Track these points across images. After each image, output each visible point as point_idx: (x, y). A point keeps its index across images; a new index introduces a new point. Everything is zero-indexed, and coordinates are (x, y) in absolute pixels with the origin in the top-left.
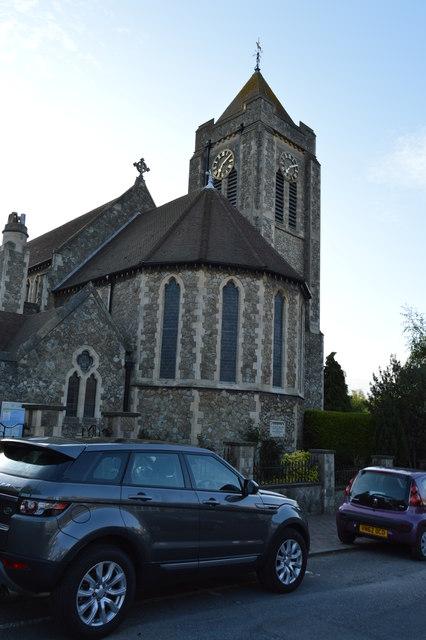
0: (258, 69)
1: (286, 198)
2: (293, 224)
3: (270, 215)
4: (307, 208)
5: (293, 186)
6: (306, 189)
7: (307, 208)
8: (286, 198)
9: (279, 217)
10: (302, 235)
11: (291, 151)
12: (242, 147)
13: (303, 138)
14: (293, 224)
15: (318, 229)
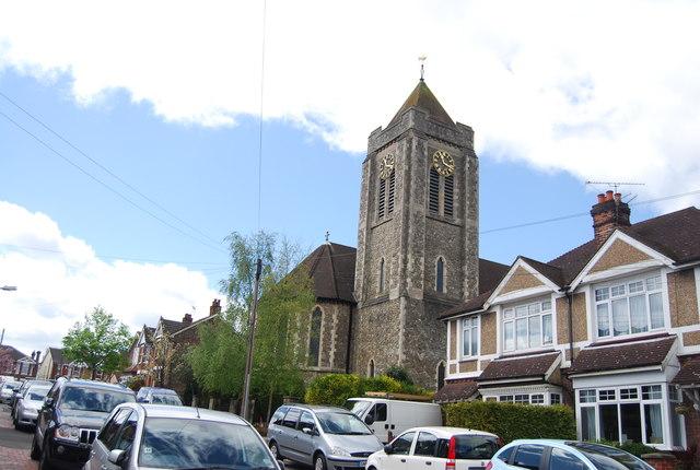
0: (422, 79)
1: (442, 194)
2: (449, 211)
3: (424, 210)
4: (462, 195)
5: (449, 180)
6: (462, 180)
7: (462, 195)
8: (442, 194)
9: (434, 206)
10: (458, 221)
11: (443, 152)
12: (397, 152)
13: (460, 137)
14: (449, 211)
15: (474, 216)
